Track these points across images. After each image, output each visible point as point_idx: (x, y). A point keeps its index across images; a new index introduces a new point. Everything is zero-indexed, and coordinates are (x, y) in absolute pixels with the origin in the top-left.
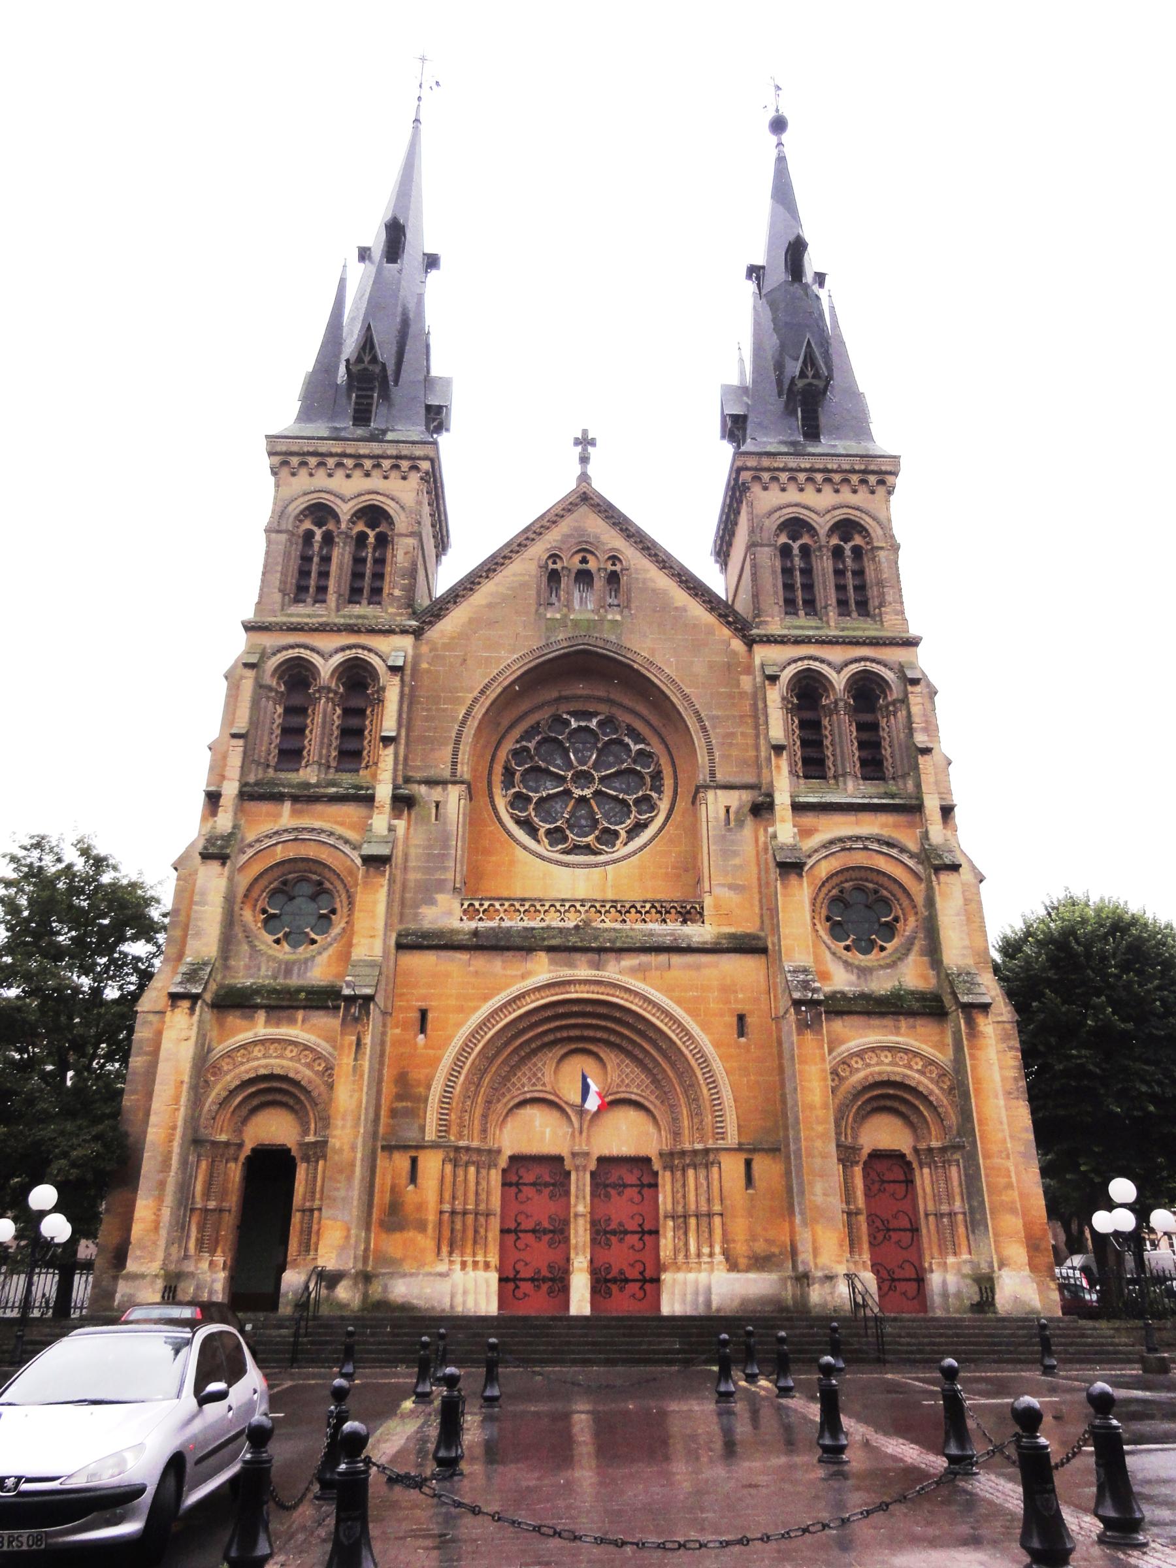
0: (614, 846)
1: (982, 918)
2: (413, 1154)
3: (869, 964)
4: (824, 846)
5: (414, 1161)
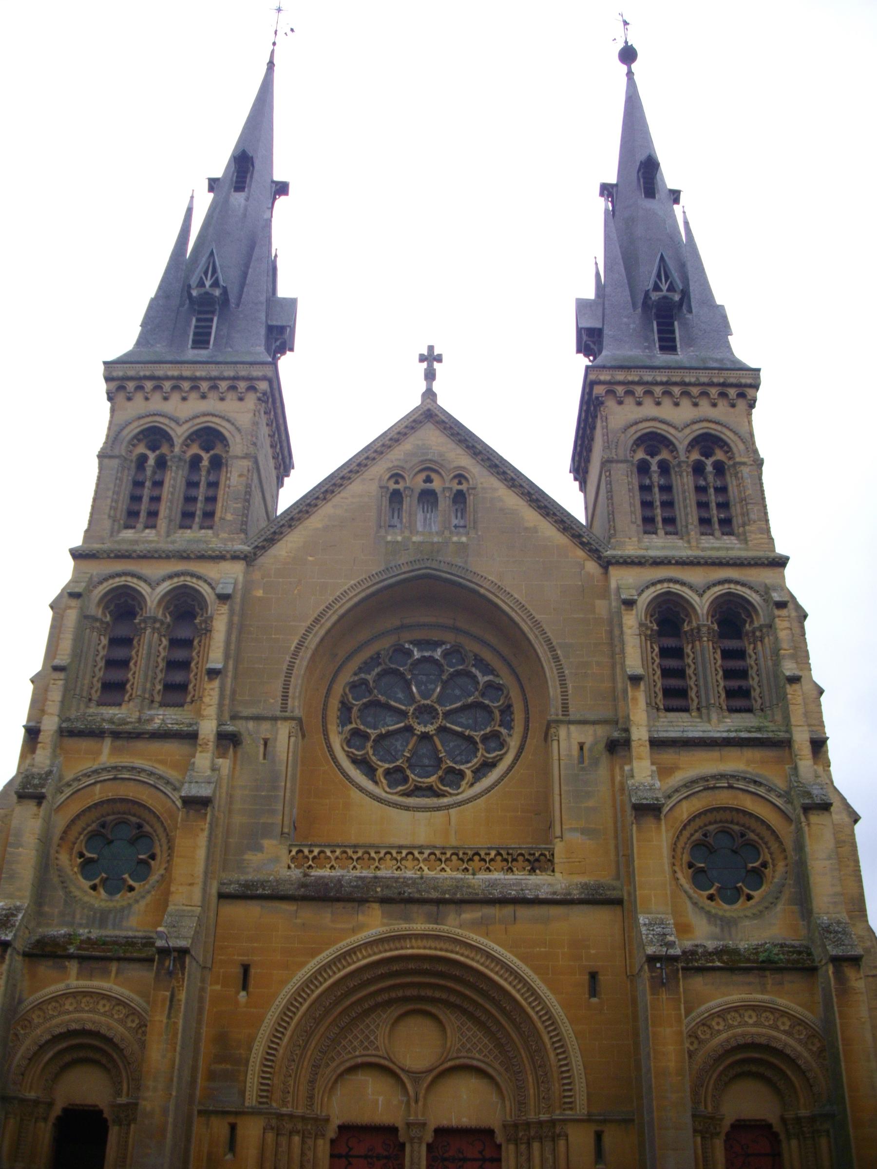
0: (459, 787)
1: (857, 862)
2: (232, 1119)
3: (734, 915)
4: (685, 786)
5: (233, 1127)
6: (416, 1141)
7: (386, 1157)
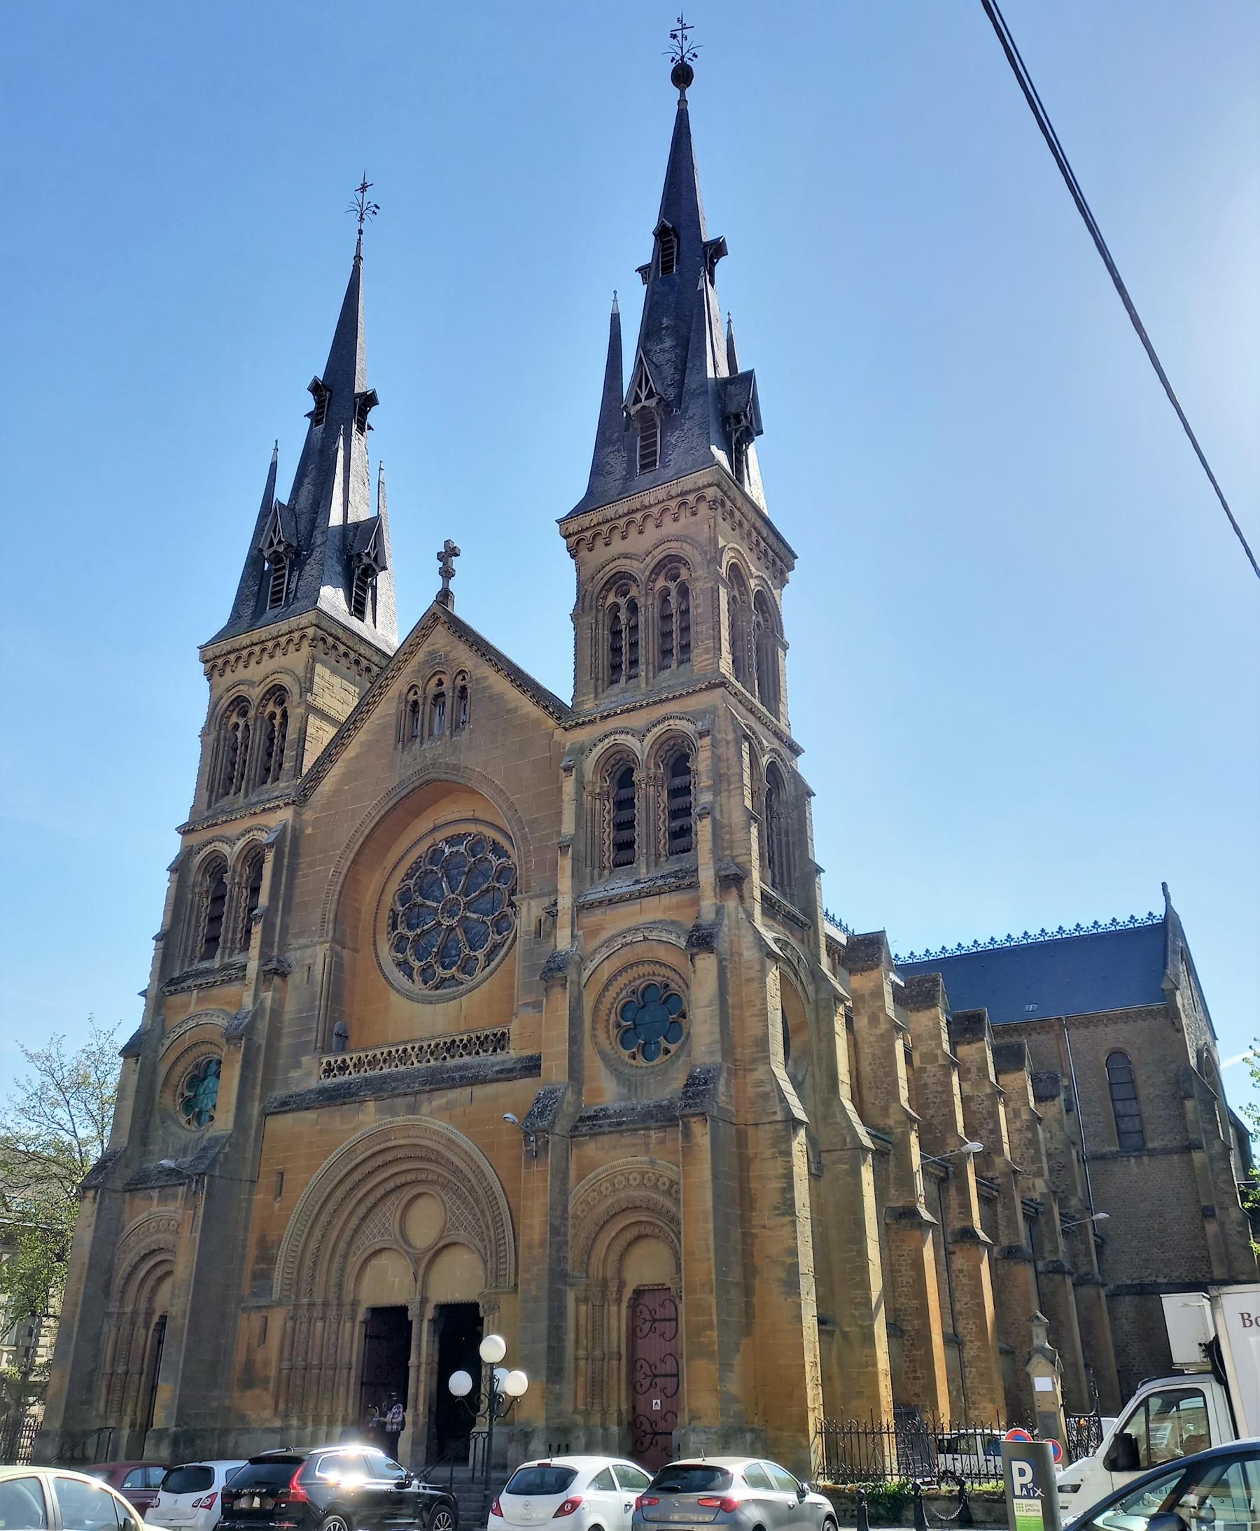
5: (266, 1318)
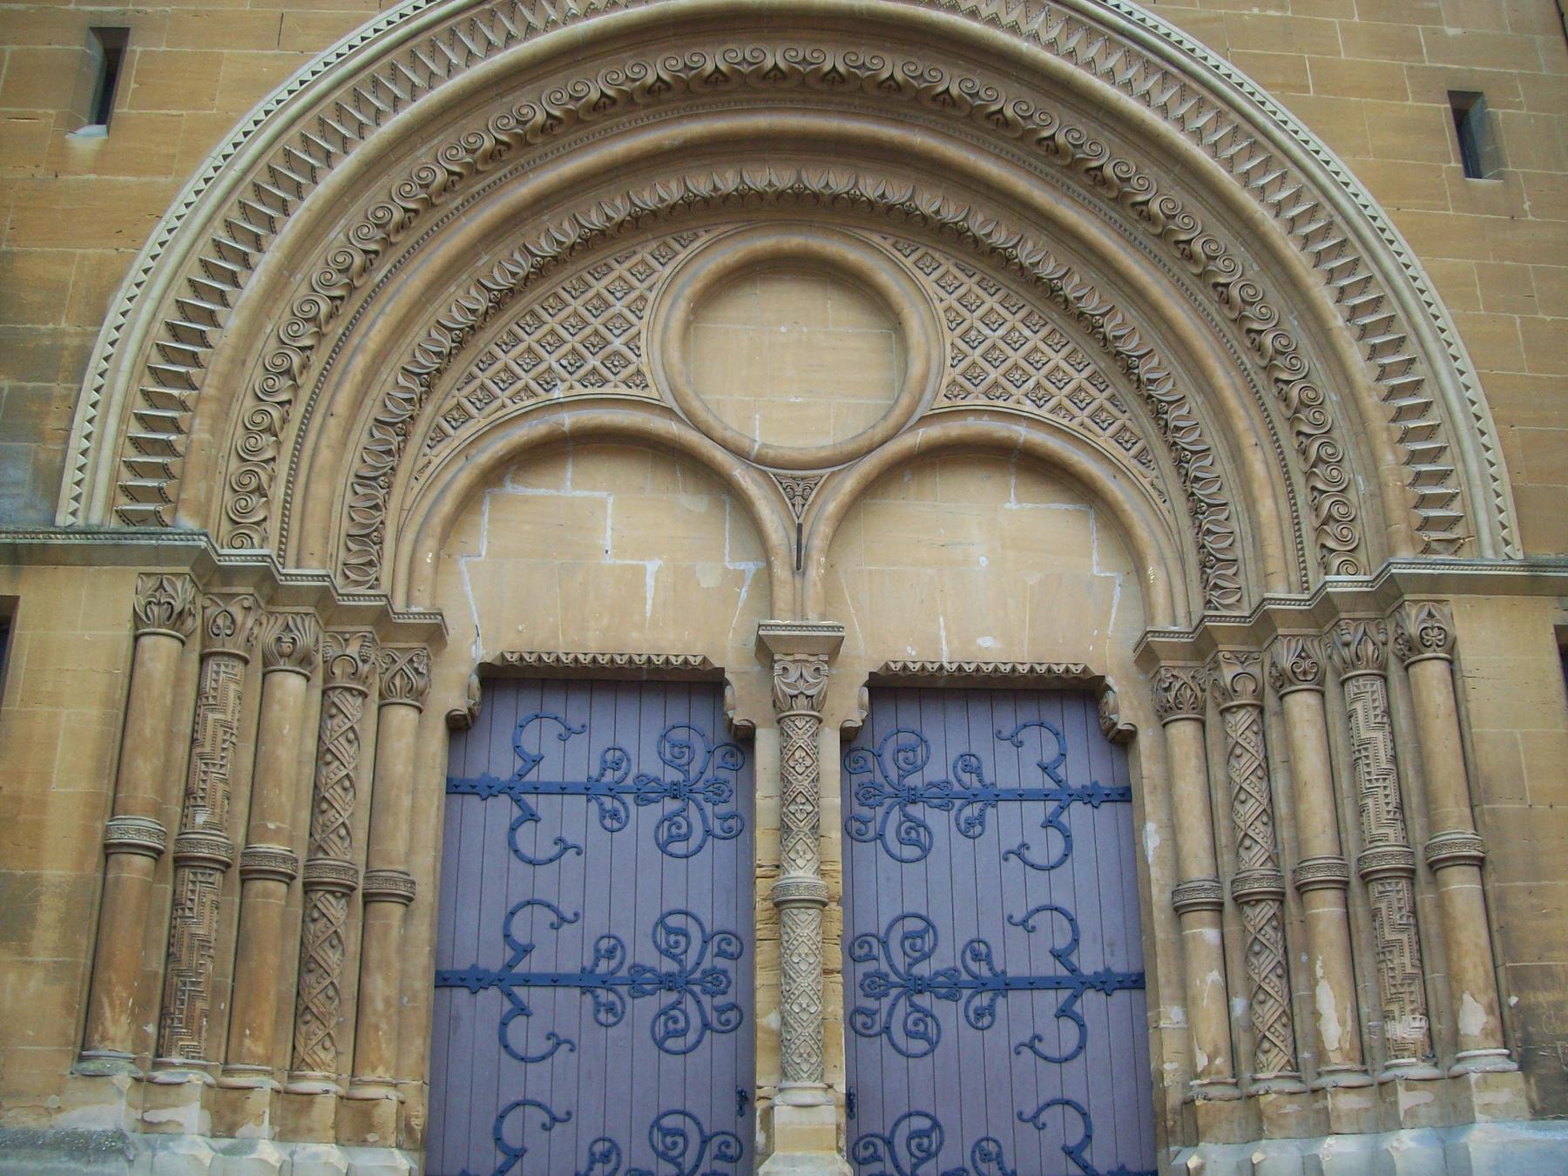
6: (801, 706)
7: (674, 792)
